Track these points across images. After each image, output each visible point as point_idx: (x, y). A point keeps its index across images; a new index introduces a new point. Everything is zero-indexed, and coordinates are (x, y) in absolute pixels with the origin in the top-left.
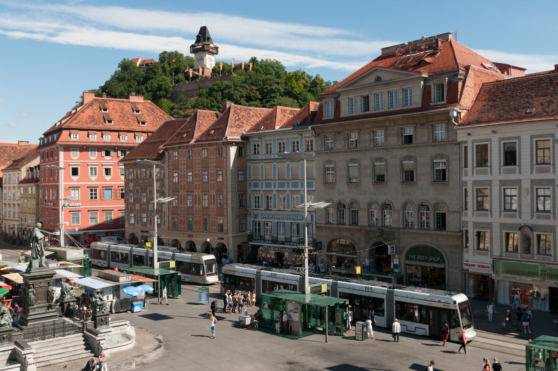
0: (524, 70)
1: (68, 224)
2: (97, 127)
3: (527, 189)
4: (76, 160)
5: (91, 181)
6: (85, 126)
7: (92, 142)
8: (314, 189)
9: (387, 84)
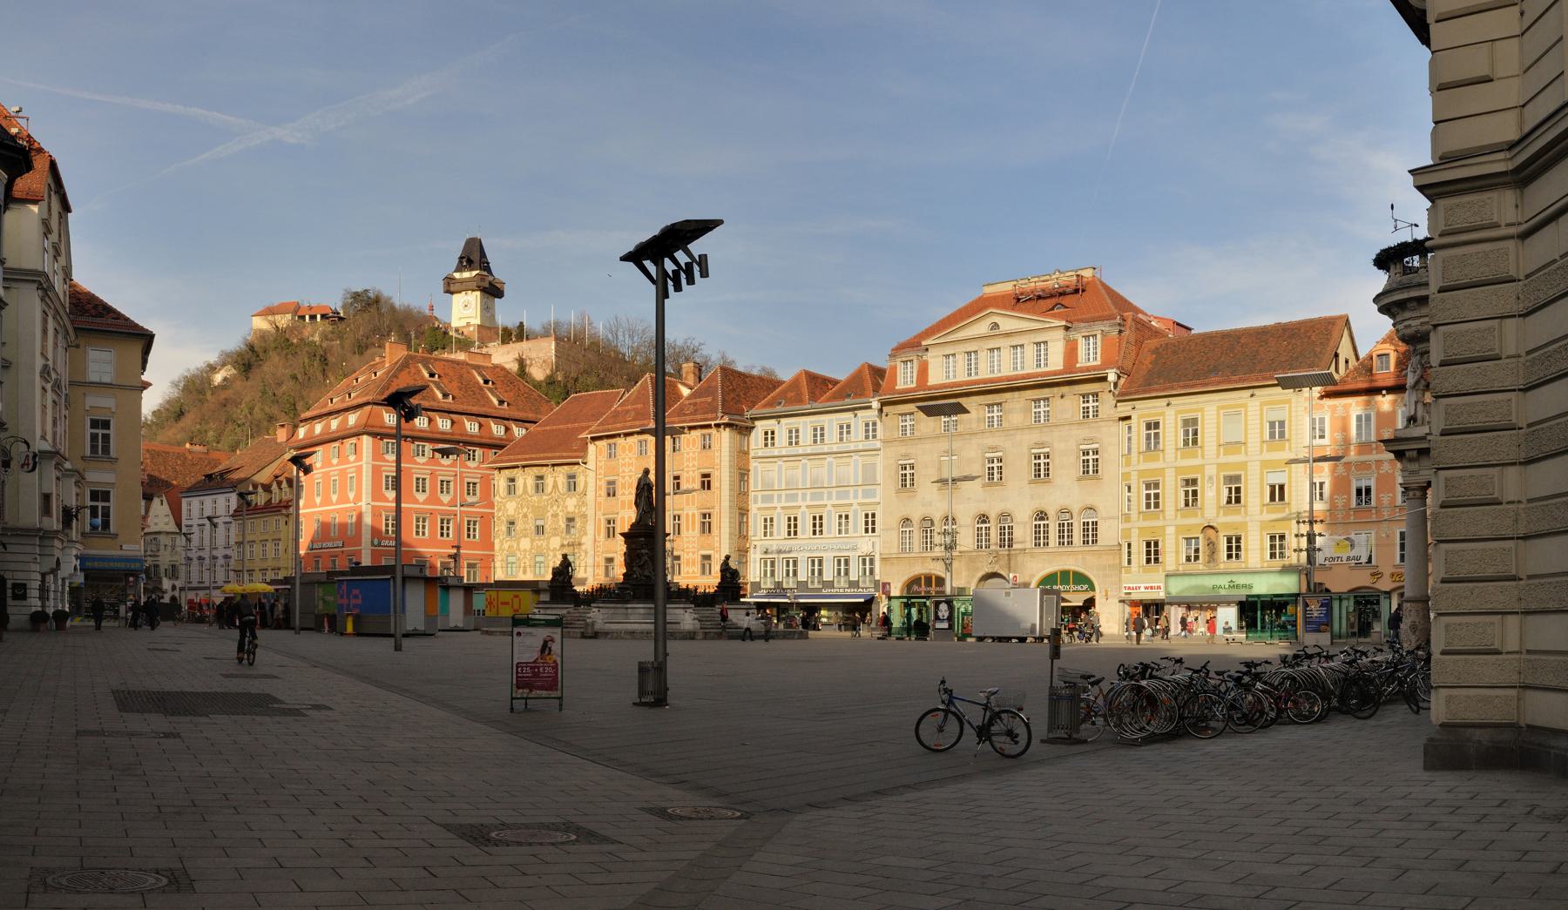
0: (1189, 329)
3: (1211, 478)
5: (417, 502)
8: (877, 500)
9: (1007, 335)
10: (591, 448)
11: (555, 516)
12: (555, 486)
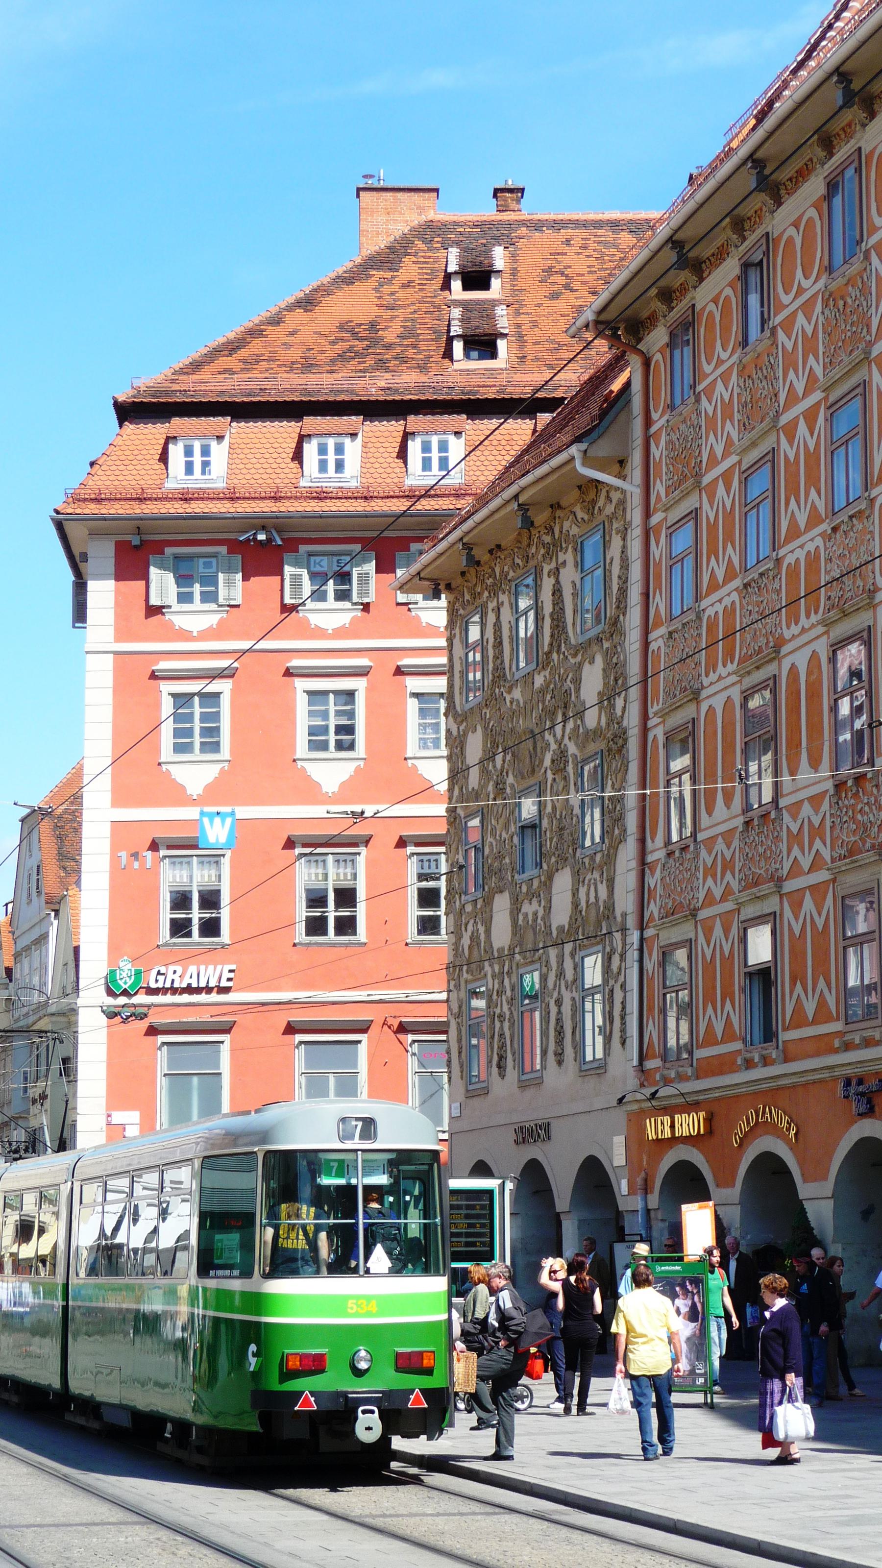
1: (132, 1131)
2: (374, 386)
4: (204, 635)
5: (310, 792)
6: (286, 385)
7: (321, 496)
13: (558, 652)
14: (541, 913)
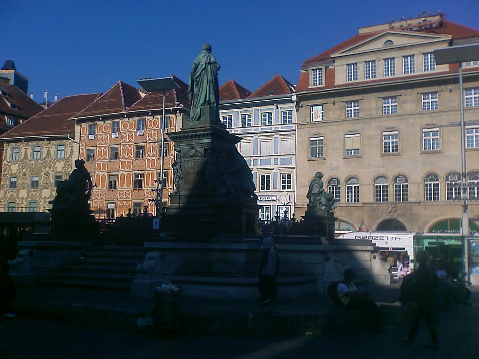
10: (77, 128)
11: (47, 174)
12: (48, 153)
13: (48, 159)
14: (38, 194)
